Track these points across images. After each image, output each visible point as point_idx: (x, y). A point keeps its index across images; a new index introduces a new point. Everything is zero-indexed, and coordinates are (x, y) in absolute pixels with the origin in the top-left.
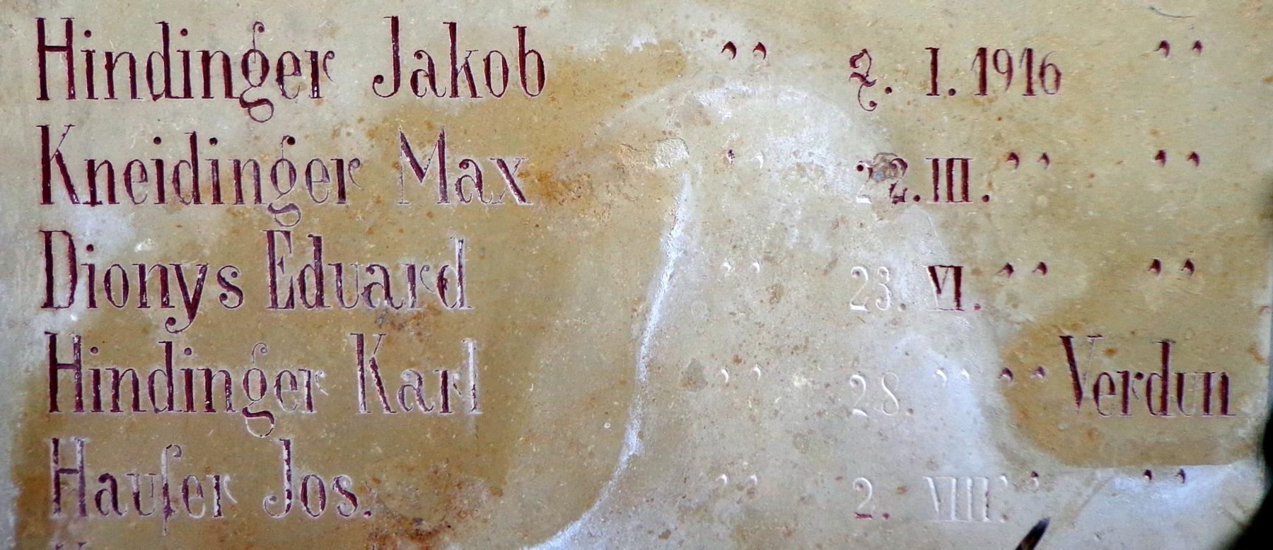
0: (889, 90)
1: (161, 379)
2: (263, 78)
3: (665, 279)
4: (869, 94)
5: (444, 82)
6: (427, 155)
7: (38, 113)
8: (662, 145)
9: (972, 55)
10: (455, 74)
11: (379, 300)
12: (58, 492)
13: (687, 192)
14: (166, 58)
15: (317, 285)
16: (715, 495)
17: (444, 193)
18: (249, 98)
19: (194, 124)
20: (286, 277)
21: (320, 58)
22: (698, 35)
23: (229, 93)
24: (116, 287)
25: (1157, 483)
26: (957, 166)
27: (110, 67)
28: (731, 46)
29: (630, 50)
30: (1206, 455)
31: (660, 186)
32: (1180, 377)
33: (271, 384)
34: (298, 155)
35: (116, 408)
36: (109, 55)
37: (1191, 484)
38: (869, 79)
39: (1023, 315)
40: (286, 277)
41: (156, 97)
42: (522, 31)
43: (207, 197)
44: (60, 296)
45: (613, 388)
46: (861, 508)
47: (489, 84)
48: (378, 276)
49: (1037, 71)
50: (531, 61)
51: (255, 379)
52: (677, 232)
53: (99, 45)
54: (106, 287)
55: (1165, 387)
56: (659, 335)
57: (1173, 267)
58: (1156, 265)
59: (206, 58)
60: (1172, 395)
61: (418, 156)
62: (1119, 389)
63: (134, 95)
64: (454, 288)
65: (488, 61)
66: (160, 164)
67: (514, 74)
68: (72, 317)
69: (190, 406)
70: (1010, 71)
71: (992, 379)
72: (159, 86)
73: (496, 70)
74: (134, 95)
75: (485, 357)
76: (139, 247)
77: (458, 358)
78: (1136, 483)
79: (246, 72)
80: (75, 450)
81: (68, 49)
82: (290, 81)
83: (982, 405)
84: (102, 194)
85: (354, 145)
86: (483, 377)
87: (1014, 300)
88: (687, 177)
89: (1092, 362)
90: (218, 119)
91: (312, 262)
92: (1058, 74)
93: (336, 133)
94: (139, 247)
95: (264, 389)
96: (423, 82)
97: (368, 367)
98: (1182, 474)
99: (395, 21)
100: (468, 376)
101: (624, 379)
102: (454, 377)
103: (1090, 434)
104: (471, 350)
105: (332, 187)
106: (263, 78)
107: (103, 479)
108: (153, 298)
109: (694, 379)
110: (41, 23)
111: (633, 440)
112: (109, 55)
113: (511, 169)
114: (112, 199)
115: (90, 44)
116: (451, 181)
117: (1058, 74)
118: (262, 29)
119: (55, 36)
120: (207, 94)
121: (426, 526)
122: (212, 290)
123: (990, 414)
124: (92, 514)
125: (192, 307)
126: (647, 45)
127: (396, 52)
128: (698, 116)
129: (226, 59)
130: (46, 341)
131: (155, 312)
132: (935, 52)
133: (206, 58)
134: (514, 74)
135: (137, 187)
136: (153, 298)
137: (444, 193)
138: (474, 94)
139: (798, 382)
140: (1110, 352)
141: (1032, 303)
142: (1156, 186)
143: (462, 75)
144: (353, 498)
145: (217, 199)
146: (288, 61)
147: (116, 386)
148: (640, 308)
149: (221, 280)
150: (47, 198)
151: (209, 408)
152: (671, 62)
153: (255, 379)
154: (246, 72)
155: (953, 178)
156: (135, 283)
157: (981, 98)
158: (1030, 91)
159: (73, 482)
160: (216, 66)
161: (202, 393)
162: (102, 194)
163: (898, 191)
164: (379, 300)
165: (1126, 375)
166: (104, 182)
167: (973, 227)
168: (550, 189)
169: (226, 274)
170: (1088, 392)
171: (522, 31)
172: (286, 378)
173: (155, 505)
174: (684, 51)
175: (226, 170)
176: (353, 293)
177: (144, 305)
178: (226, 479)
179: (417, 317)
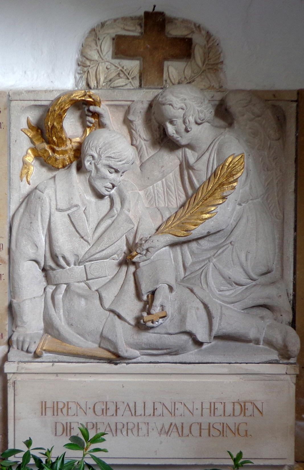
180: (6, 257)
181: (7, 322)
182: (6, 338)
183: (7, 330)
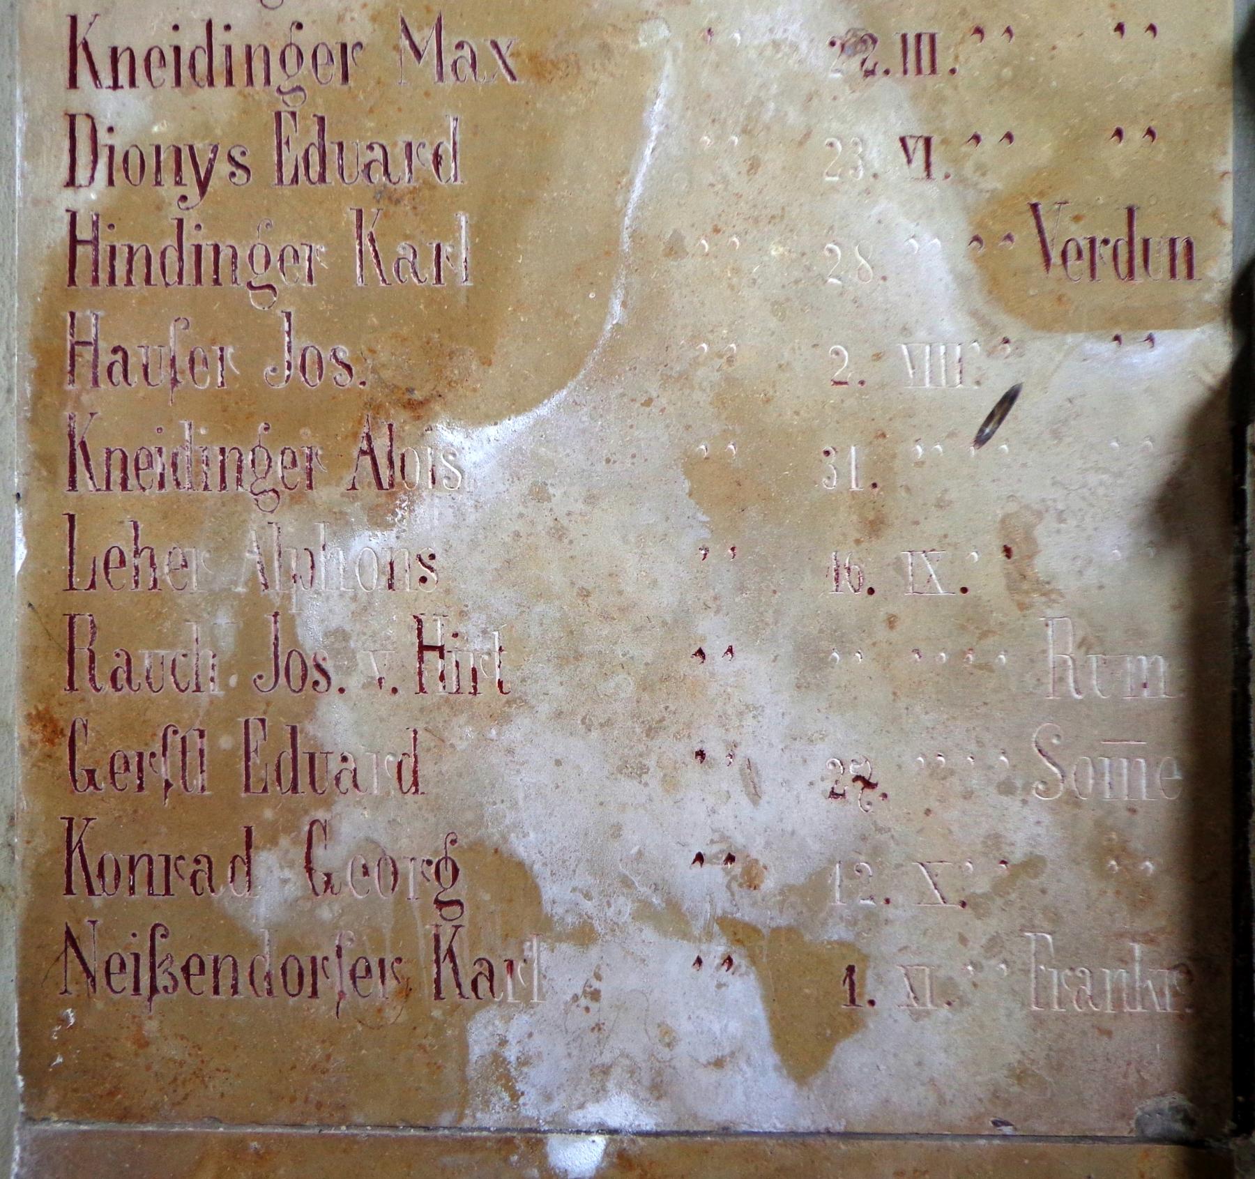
1: (172, 255)
3: (648, 152)
6: (425, 37)
8: (645, 26)
11: (378, 175)
12: (73, 365)
13: (668, 68)
16: (695, 363)
20: (291, 156)
24: (130, 167)
25: (1127, 348)
26: (925, 41)
30: (1175, 319)
31: (644, 64)
32: (1146, 242)
33: (274, 258)
34: (306, 40)
35: (129, 282)
37: (1159, 350)
39: (992, 183)
40: (291, 156)
43: (220, 80)
44: (82, 175)
45: (596, 259)
46: (837, 375)
48: (378, 153)
51: (259, 253)
52: (659, 106)
55: (1131, 252)
56: (641, 207)
57: (1135, 135)
58: (1119, 133)
60: (1138, 261)
62: (1086, 254)
64: (449, 166)
66: (177, 50)
69: (199, 280)
71: (962, 245)
75: (475, 230)
76: (156, 129)
77: (453, 231)
78: (1106, 348)
83: (952, 271)
84: (123, 78)
86: (475, 250)
87: (982, 169)
88: (668, 54)
89: (1060, 228)
91: (316, 140)
94: (156, 129)
95: (268, 262)
97: (366, 240)
98: (1150, 339)
100: (460, 248)
101: (608, 250)
102: (447, 249)
103: (1060, 299)
104: (463, 224)
107: (115, 351)
108: (168, 177)
109: (675, 249)
111: (617, 308)
114: (132, 83)
121: (418, 396)
123: (962, 281)
124: (104, 385)
125: (203, 185)
130: (67, 217)
131: (169, 190)
135: (155, 72)
136: (168, 177)
139: (775, 251)
140: (1077, 219)
141: (999, 171)
142: (1117, 58)
144: (348, 368)
145: (230, 82)
147: (130, 261)
149: (231, 159)
150: (73, 82)
151: (216, 282)
153: (259, 253)
156: (151, 163)
159: (87, 354)
161: (209, 268)
162: (123, 78)
163: (869, 65)
164: (378, 175)
165: (1092, 241)
166: (126, 67)
167: (939, 99)
168: (540, 68)
169: (236, 154)
170: (1056, 258)
172: (289, 253)
173: (162, 377)
175: (239, 54)
176: (354, 169)
177: (158, 183)
178: (229, 351)
181: (1227, 162)
183: (1228, 215)
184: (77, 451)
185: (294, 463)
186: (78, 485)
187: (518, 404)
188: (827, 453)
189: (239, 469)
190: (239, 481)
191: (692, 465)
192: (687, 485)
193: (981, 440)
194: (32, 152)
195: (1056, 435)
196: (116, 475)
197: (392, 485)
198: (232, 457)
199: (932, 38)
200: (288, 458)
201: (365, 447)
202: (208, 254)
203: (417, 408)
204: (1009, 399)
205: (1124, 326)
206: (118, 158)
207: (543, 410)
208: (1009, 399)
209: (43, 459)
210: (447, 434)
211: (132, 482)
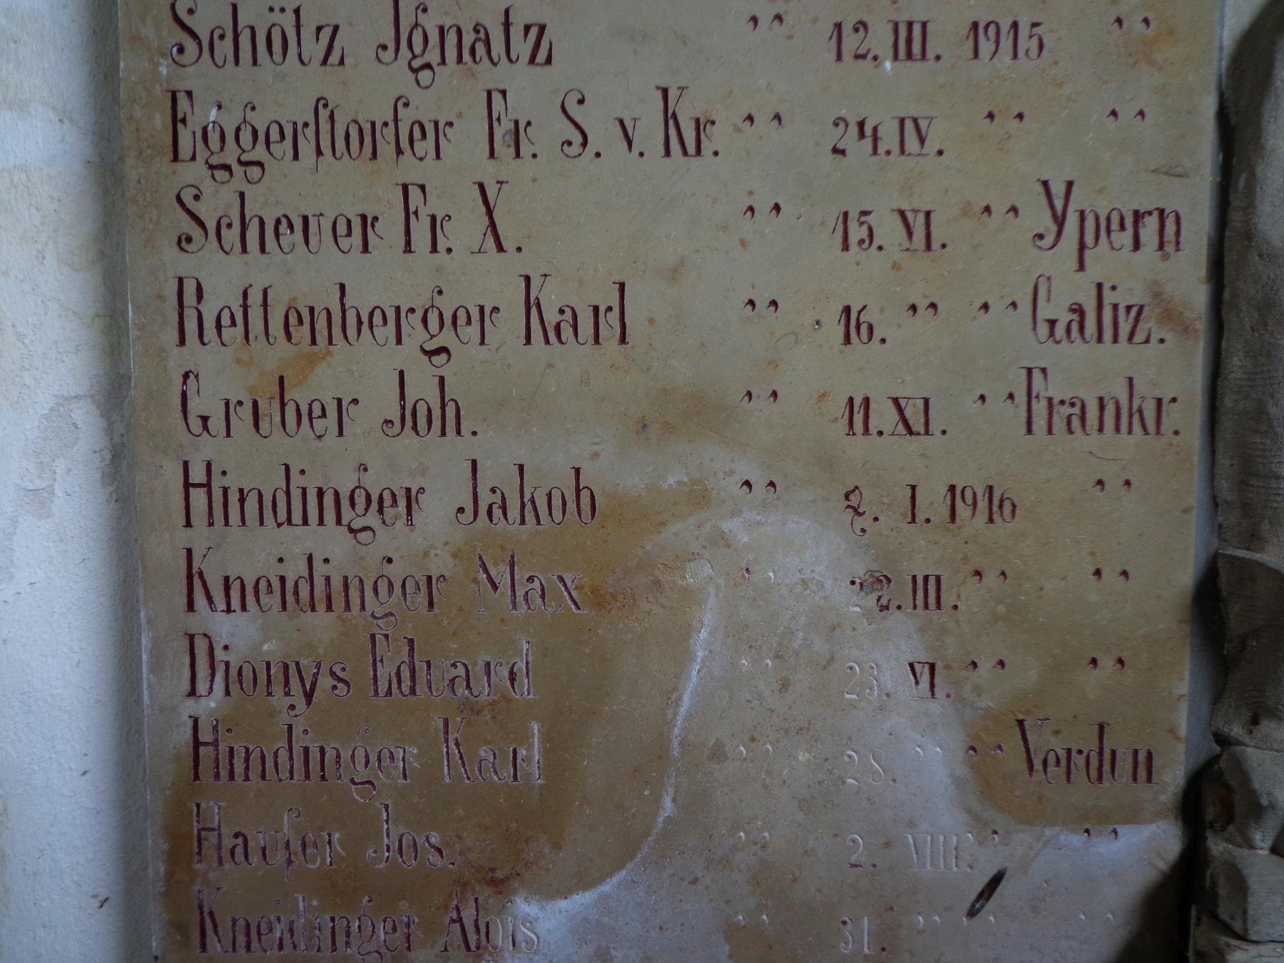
0: (876, 519)
1: (283, 754)
2: (366, 510)
3: (694, 673)
4: (860, 523)
5: (514, 512)
6: (500, 572)
7: (183, 537)
9: (943, 490)
10: (523, 506)
11: (461, 691)
12: (200, 846)
13: (712, 602)
14: (288, 493)
15: (411, 677)
17: (514, 603)
18: (355, 526)
19: (310, 546)
20: (385, 671)
21: (413, 493)
22: (721, 475)
23: (339, 522)
24: (242, 680)
26: (932, 581)
27: (242, 500)
28: (747, 483)
29: (665, 486)
30: (1134, 816)
31: (690, 597)
32: (1113, 753)
33: (373, 758)
35: (247, 778)
36: (241, 491)
37: (1122, 840)
38: (861, 510)
39: (986, 702)
40: (385, 671)
41: (279, 525)
42: (578, 471)
43: (321, 607)
44: (202, 687)
46: (853, 859)
47: (550, 514)
48: (461, 671)
49: (997, 504)
50: (585, 496)
51: (360, 754)
52: (704, 634)
53: (233, 482)
54: (236, 679)
56: (689, 718)
57: (1107, 663)
58: (1094, 661)
59: (320, 493)
60: (1107, 767)
61: (493, 572)
62: (1063, 762)
63: (262, 523)
65: (549, 495)
66: (282, 579)
67: (571, 506)
68: (211, 704)
69: (307, 776)
70: (975, 504)
72: (282, 516)
73: (557, 502)
74: (262, 523)
75: (546, 737)
76: (266, 647)
77: (526, 739)
78: (1078, 839)
79: (353, 505)
80: (214, 811)
81: (208, 486)
82: (389, 512)
84: (235, 603)
85: (441, 564)
86: (546, 753)
87: (978, 690)
89: (1042, 740)
90: (331, 543)
91: (406, 659)
92: (1014, 506)
93: (426, 554)
94: (266, 647)
96: (497, 513)
97: (452, 745)
98: (1115, 832)
99: (474, 463)
100: (534, 752)
102: (522, 752)
103: (1040, 799)
104: (536, 731)
105: (422, 598)
106: (366, 510)
107: (236, 836)
108: (278, 689)
109: (717, 754)
110: (186, 464)
111: (668, 805)
112: (241, 491)
113: (569, 584)
114: (244, 608)
115: (226, 482)
116: (520, 593)
117: (1014, 506)
118: (365, 470)
119: (198, 475)
120: (321, 522)
121: (499, 874)
122: (325, 682)
123: (958, 782)
124: (228, 866)
125: (309, 696)
126: (680, 483)
127: (475, 487)
128: (721, 540)
129: (337, 494)
130: (190, 723)
131: (279, 700)
132: (913, 488)
133: (320, 493)
134: (571, 506)
135: (264, 599)
136: (278, 689)
137: (514, 603)
138: (539, 522)
139: (802, 757)
140: (1057, 733)
143: (529, 507)
144: (439, 851)
146: (387, 495)
147: (247, 760)
148: (674, 697)
149: (333, 674)
150: (191, 607)
151: (323, 778)
152: (698, 497)
153: (360, 754)
154: (353, 505)
155: (928, 592)
156: (262, 677)
157: (951, 526)
158: (991, 520)
160: (329, 500)
161: (318, 767)
162: (235, 603)
163: (884, 602)
164: (461, 691)
165: (1069, 751)
166: (237, 594)
168: (600, 599)
169: (337, 669)
170: (1038, 765)
171: (578, 471)
172: (386, 753)
173: (279, 857)
174: (709, 487)
175: (337, 584)
177: (270, 694)
178: (336, 836)
179: (493, 704)
180: (1198, 297)
182: (1173, 777)
183: (1183, 731)
184: (206, 922)
185: (394, 929)
186: (208, 947)
187: (585, 881)
188: (844, 923)
189: (348, 935)
190: (348, 944)
191: (732, 932)
192: (727, 949)
193: (972, 913)
194: (156, 667)
195: (1034, 909)
196: (241, 939)
197: (478, 948)
198: (341, 925)
199: (938, 579)
200: (389, 925)
201: (455, 916)
202: (315, 755)
203: (500, 885)
204: (996, 880)
205: (1092, 821)
206: (233, 672)
207: (606, 888)
208: (996, 880)
209: (177, 927)
210: (524, 907)
211: (255, 945)
